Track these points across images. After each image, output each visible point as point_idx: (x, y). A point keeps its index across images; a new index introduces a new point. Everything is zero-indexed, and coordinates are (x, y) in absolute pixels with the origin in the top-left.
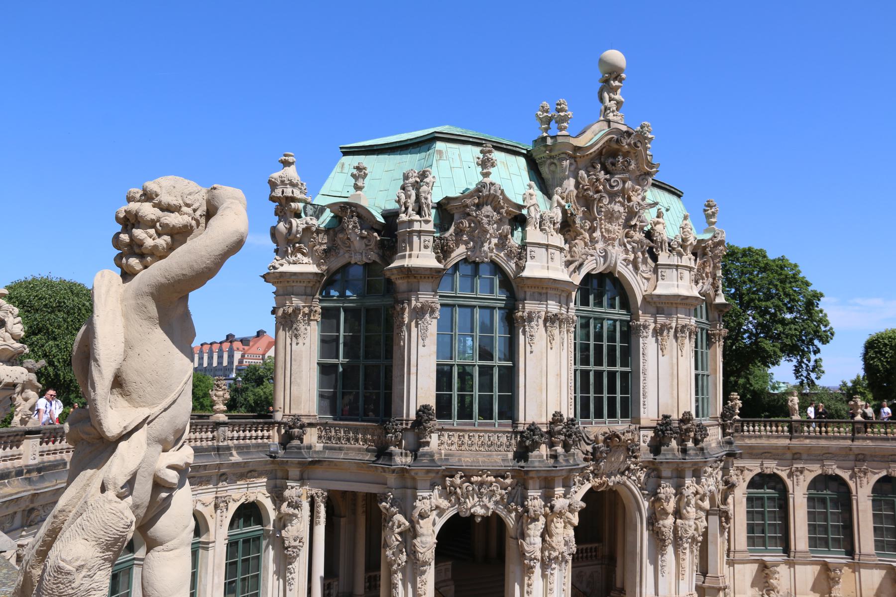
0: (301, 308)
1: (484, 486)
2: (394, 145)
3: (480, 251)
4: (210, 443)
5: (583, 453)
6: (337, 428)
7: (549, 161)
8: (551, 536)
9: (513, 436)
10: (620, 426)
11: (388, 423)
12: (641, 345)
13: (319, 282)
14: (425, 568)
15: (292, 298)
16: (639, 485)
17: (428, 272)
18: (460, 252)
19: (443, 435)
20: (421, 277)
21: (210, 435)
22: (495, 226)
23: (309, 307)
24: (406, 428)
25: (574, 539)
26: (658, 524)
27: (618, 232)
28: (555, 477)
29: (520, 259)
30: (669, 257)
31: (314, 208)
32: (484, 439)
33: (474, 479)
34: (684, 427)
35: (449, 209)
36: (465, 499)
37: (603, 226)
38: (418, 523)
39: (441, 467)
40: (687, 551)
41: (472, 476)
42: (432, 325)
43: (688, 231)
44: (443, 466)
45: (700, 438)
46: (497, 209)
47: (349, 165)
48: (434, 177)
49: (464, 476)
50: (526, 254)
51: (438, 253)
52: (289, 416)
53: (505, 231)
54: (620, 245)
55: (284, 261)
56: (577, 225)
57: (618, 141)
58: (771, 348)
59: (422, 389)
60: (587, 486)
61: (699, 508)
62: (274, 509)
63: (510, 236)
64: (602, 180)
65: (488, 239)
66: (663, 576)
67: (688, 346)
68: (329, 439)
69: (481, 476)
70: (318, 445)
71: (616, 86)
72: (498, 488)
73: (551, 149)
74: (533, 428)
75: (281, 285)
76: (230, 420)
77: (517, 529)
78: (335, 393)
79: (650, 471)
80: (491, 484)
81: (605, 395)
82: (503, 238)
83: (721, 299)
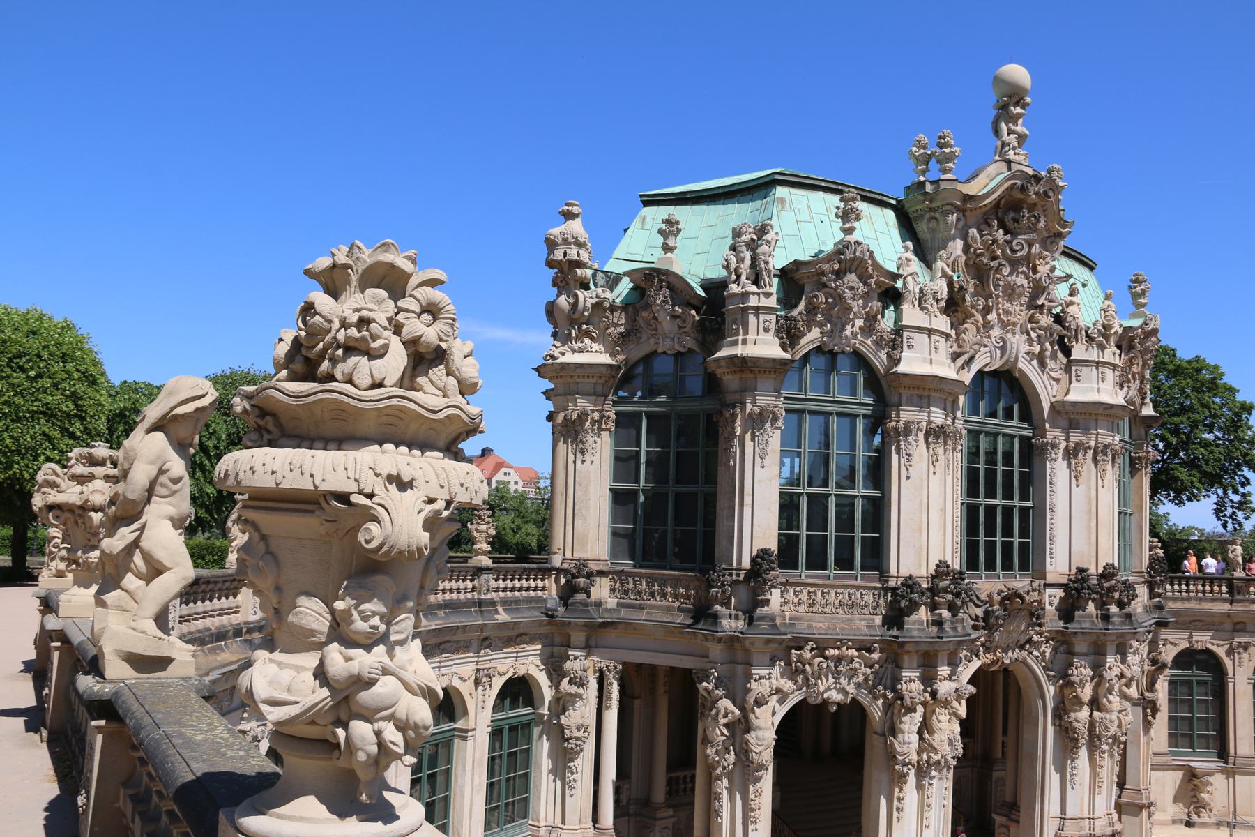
0: (590, 412)
1: (843, 662)
2: (715, 192)
3: (841, 337)
4: (469, 596)
5: (971, 619)
6: (637, 579)
7: (928, 216)
8: (931, 732)
9: (882, 594)
10: (1020, 582)
11: (711, 572)
12: (1048, 471)
13: (614, 377)
14: (760, 773)
15: (576, 399)
16: (1043, 664)
17: (770, 365)
18: (812, 337)
19: (788, 591)
20: (759, 371)
21: (469, 584)
23: (600, 411)
24: (737, 580)
25: (959, 737)
26: (1069, 717)
28: (939, 651)
29: (894, 348)
30: (1087, 350)
31: (607, 276)
33: (829, 652)
34: (1106, 585)
36: (816, 680)
37: (1000, 306)
38: (753, 712)
41: (826, 648)
42: (774, 438)
43: (1112, 315)
45: (1126, 600)
46: (864, 278)
47: (653, 219)
48: (777, 233)
49: (816, 648)
50: (902, 342)
51: (783, 338)
52: (572, 560)
53: (875, 309)
54: (1022, 333)
55: (566, 348)
56: (967, 304)
57: (1023, 189)
58: (1187, 478)
59: (759, 526)
60: (976, 664)
61: (1124, 696)
62: (549, 686)
63: (879, 317)
64: (1001, 242)
65: (851, 320)
66: (1073, 788)
67: (1111, 473)
68: (626, 592)
69: (839, 648)
70: (610, 600)
71: (1018, 114)
72: (861, 665)
73: (930, 197)
74: (910, 583)
75: (561, 381)
76: (495, 565)
77: (885, 722)
78: (634, 529)
79: (1058, 644)
81: (999, 539)
82: (871, 320)
83: (1148, 411)
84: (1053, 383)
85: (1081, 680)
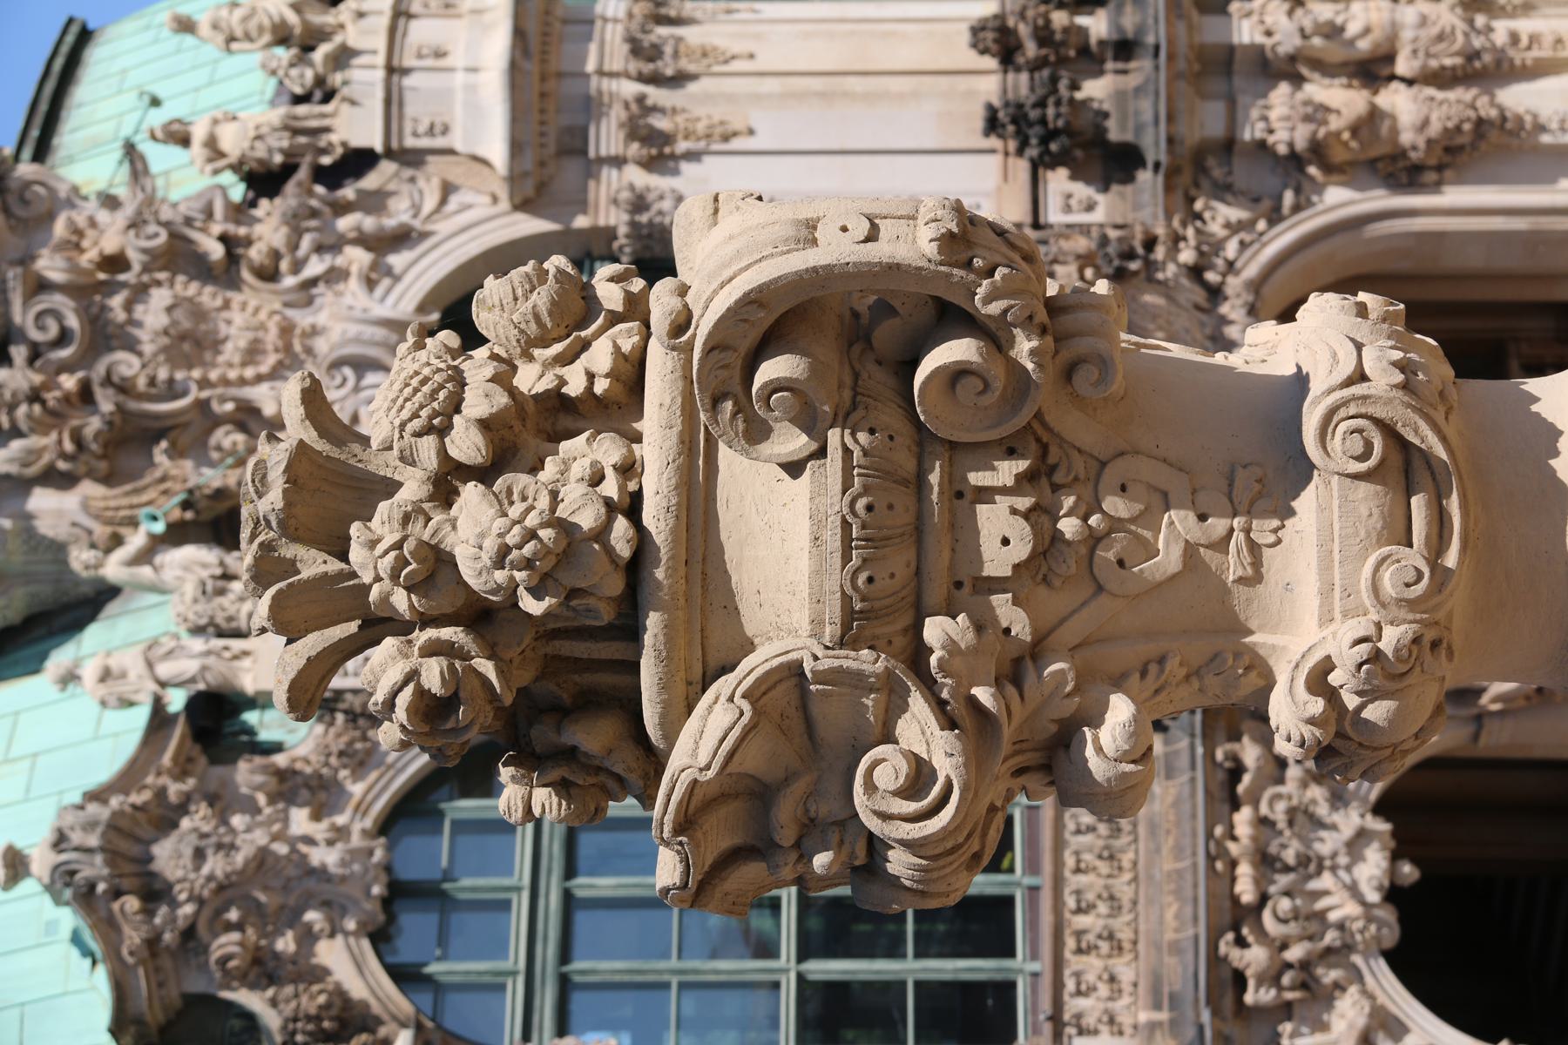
1: (1273, 849)
19: (1078, 1016)
22: (238, 821)
27: (257, 310)
30: (353, 103)
32: (1090, 850)
33: (1245, 890)
34: (1031, 49)
35: (161, 1017)
39: (1201, 1028)
40: (1525, 26)
41: (1235, 900)
44: (1198, 1015)
46: (165, 817)
49: (1236, 928)
53: (259, 779)
54: (309, 302)
63: (280, 760)
65: (294, 850)
69: (1233, 864)
72: (1278, 796)
79: (1205, 183)
80: (1264, 822)
84: (454, 201)
85: (1307, 119)
